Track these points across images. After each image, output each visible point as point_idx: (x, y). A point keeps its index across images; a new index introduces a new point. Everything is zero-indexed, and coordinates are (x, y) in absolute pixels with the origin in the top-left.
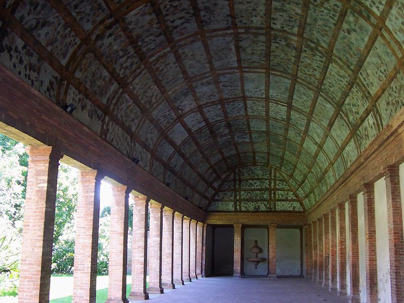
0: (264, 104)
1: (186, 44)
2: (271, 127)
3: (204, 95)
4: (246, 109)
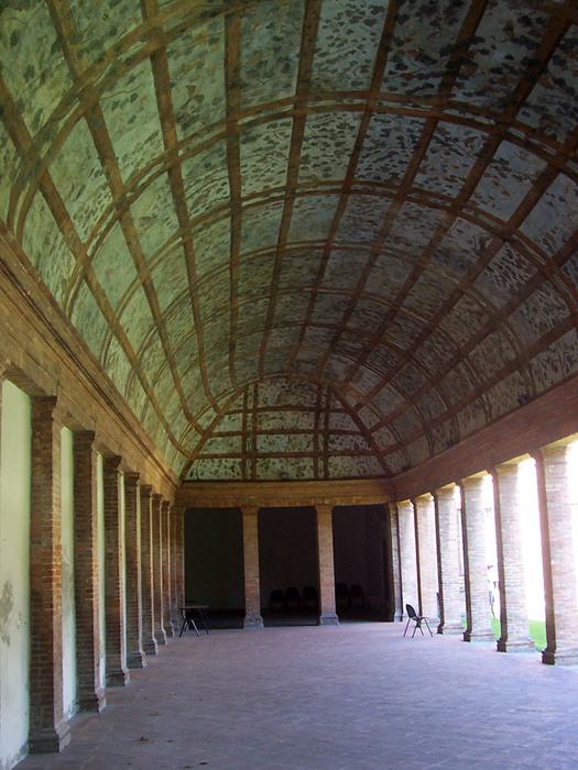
0: (301, 173)
1: (383, 298)
2: (294, 54)
3: (422, 226)
4: (358, 147)
